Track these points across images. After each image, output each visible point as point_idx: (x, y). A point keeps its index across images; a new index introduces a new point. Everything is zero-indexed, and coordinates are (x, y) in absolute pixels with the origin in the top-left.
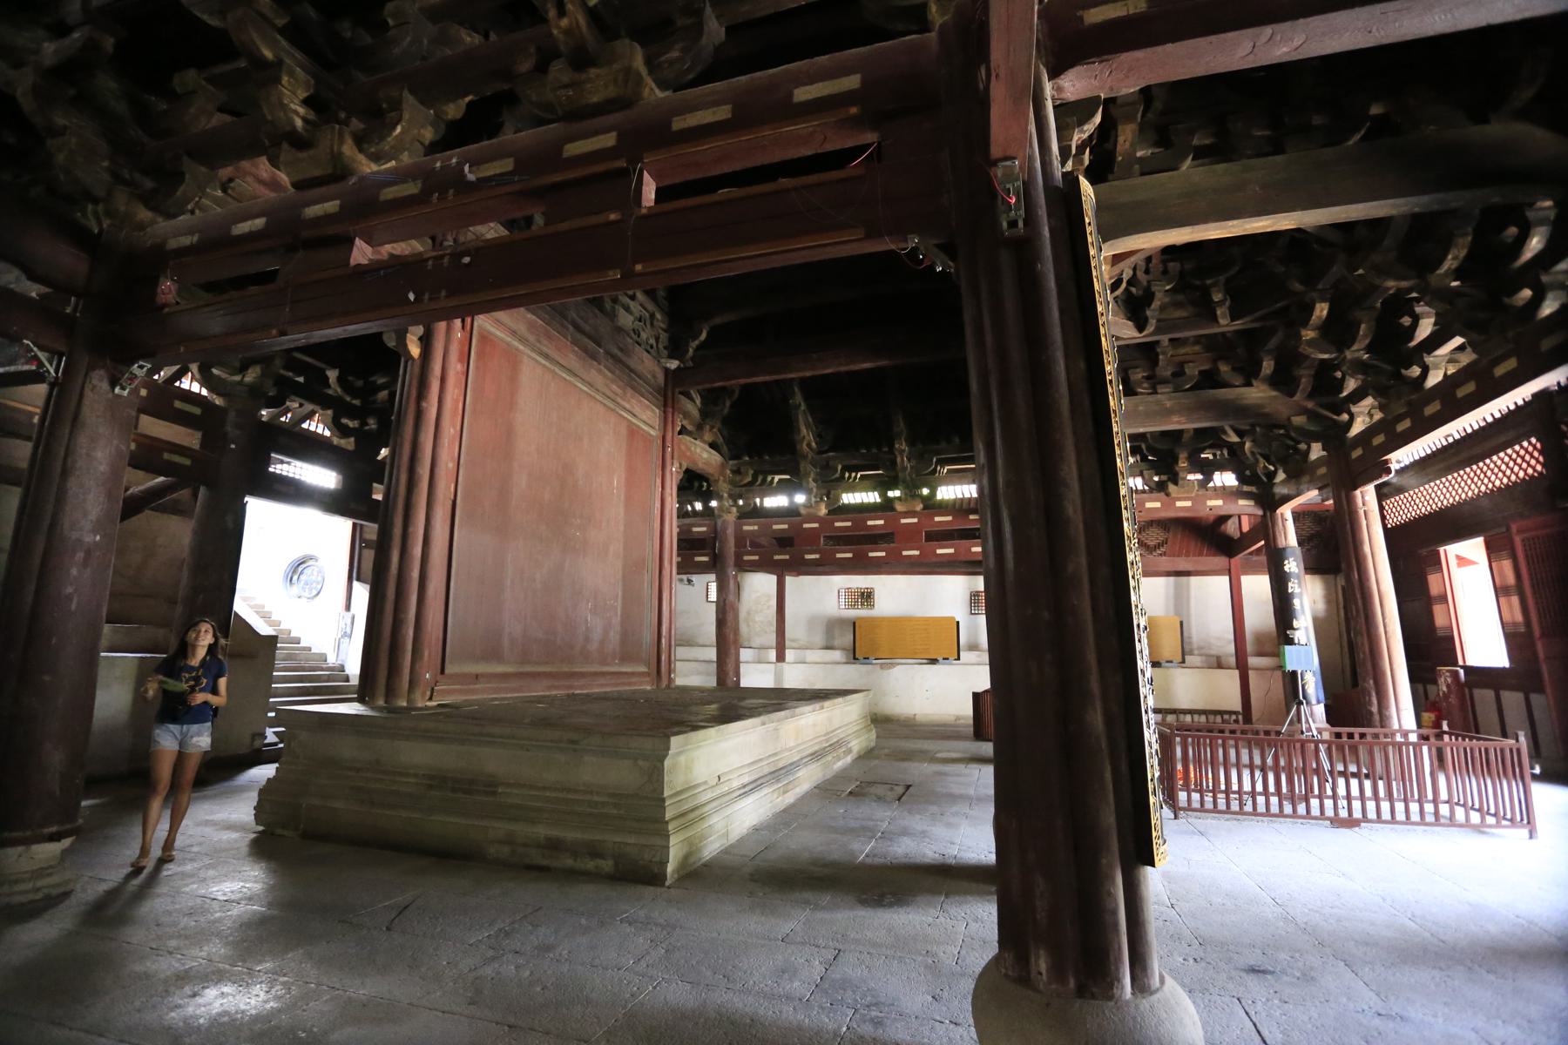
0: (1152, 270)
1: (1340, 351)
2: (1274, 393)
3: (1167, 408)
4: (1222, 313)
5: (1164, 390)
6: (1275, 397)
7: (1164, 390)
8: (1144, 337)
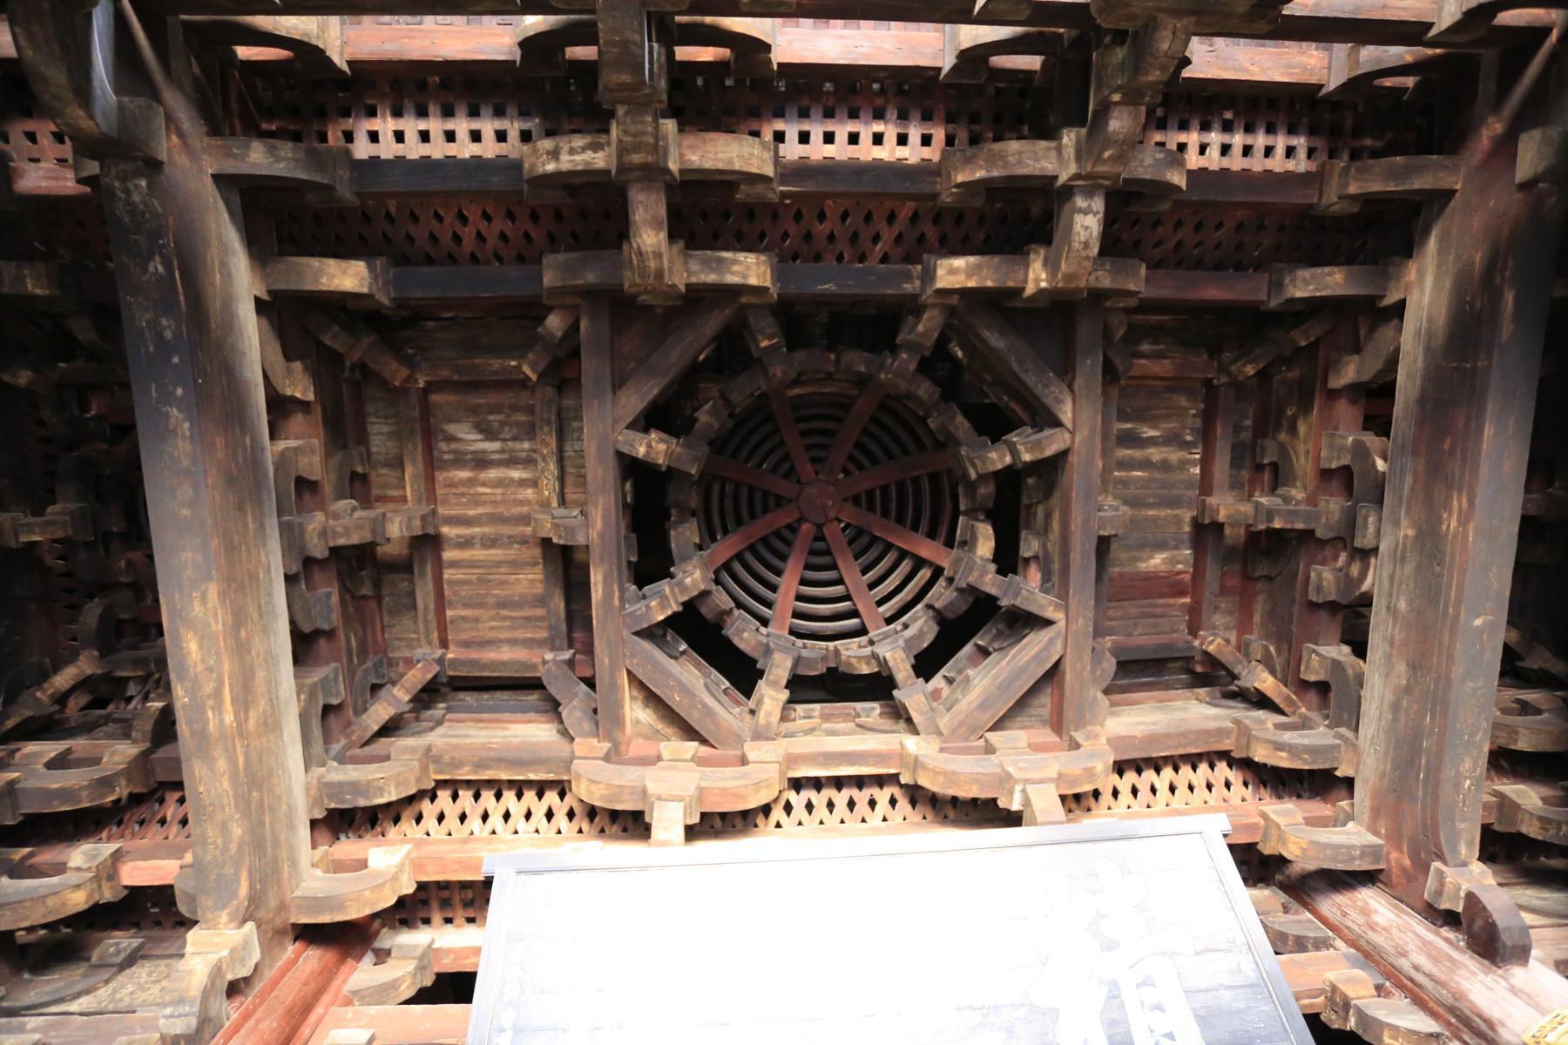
0: (951, 574)
1: (1067, 192)
2: (1432, 244)
3: (1416, 537)
4: (1028, 450)
5: (1371, 529)
6: (1444, 239)
7: (1371, 529)
8: (1067, 615)
